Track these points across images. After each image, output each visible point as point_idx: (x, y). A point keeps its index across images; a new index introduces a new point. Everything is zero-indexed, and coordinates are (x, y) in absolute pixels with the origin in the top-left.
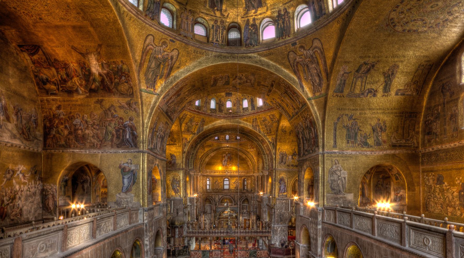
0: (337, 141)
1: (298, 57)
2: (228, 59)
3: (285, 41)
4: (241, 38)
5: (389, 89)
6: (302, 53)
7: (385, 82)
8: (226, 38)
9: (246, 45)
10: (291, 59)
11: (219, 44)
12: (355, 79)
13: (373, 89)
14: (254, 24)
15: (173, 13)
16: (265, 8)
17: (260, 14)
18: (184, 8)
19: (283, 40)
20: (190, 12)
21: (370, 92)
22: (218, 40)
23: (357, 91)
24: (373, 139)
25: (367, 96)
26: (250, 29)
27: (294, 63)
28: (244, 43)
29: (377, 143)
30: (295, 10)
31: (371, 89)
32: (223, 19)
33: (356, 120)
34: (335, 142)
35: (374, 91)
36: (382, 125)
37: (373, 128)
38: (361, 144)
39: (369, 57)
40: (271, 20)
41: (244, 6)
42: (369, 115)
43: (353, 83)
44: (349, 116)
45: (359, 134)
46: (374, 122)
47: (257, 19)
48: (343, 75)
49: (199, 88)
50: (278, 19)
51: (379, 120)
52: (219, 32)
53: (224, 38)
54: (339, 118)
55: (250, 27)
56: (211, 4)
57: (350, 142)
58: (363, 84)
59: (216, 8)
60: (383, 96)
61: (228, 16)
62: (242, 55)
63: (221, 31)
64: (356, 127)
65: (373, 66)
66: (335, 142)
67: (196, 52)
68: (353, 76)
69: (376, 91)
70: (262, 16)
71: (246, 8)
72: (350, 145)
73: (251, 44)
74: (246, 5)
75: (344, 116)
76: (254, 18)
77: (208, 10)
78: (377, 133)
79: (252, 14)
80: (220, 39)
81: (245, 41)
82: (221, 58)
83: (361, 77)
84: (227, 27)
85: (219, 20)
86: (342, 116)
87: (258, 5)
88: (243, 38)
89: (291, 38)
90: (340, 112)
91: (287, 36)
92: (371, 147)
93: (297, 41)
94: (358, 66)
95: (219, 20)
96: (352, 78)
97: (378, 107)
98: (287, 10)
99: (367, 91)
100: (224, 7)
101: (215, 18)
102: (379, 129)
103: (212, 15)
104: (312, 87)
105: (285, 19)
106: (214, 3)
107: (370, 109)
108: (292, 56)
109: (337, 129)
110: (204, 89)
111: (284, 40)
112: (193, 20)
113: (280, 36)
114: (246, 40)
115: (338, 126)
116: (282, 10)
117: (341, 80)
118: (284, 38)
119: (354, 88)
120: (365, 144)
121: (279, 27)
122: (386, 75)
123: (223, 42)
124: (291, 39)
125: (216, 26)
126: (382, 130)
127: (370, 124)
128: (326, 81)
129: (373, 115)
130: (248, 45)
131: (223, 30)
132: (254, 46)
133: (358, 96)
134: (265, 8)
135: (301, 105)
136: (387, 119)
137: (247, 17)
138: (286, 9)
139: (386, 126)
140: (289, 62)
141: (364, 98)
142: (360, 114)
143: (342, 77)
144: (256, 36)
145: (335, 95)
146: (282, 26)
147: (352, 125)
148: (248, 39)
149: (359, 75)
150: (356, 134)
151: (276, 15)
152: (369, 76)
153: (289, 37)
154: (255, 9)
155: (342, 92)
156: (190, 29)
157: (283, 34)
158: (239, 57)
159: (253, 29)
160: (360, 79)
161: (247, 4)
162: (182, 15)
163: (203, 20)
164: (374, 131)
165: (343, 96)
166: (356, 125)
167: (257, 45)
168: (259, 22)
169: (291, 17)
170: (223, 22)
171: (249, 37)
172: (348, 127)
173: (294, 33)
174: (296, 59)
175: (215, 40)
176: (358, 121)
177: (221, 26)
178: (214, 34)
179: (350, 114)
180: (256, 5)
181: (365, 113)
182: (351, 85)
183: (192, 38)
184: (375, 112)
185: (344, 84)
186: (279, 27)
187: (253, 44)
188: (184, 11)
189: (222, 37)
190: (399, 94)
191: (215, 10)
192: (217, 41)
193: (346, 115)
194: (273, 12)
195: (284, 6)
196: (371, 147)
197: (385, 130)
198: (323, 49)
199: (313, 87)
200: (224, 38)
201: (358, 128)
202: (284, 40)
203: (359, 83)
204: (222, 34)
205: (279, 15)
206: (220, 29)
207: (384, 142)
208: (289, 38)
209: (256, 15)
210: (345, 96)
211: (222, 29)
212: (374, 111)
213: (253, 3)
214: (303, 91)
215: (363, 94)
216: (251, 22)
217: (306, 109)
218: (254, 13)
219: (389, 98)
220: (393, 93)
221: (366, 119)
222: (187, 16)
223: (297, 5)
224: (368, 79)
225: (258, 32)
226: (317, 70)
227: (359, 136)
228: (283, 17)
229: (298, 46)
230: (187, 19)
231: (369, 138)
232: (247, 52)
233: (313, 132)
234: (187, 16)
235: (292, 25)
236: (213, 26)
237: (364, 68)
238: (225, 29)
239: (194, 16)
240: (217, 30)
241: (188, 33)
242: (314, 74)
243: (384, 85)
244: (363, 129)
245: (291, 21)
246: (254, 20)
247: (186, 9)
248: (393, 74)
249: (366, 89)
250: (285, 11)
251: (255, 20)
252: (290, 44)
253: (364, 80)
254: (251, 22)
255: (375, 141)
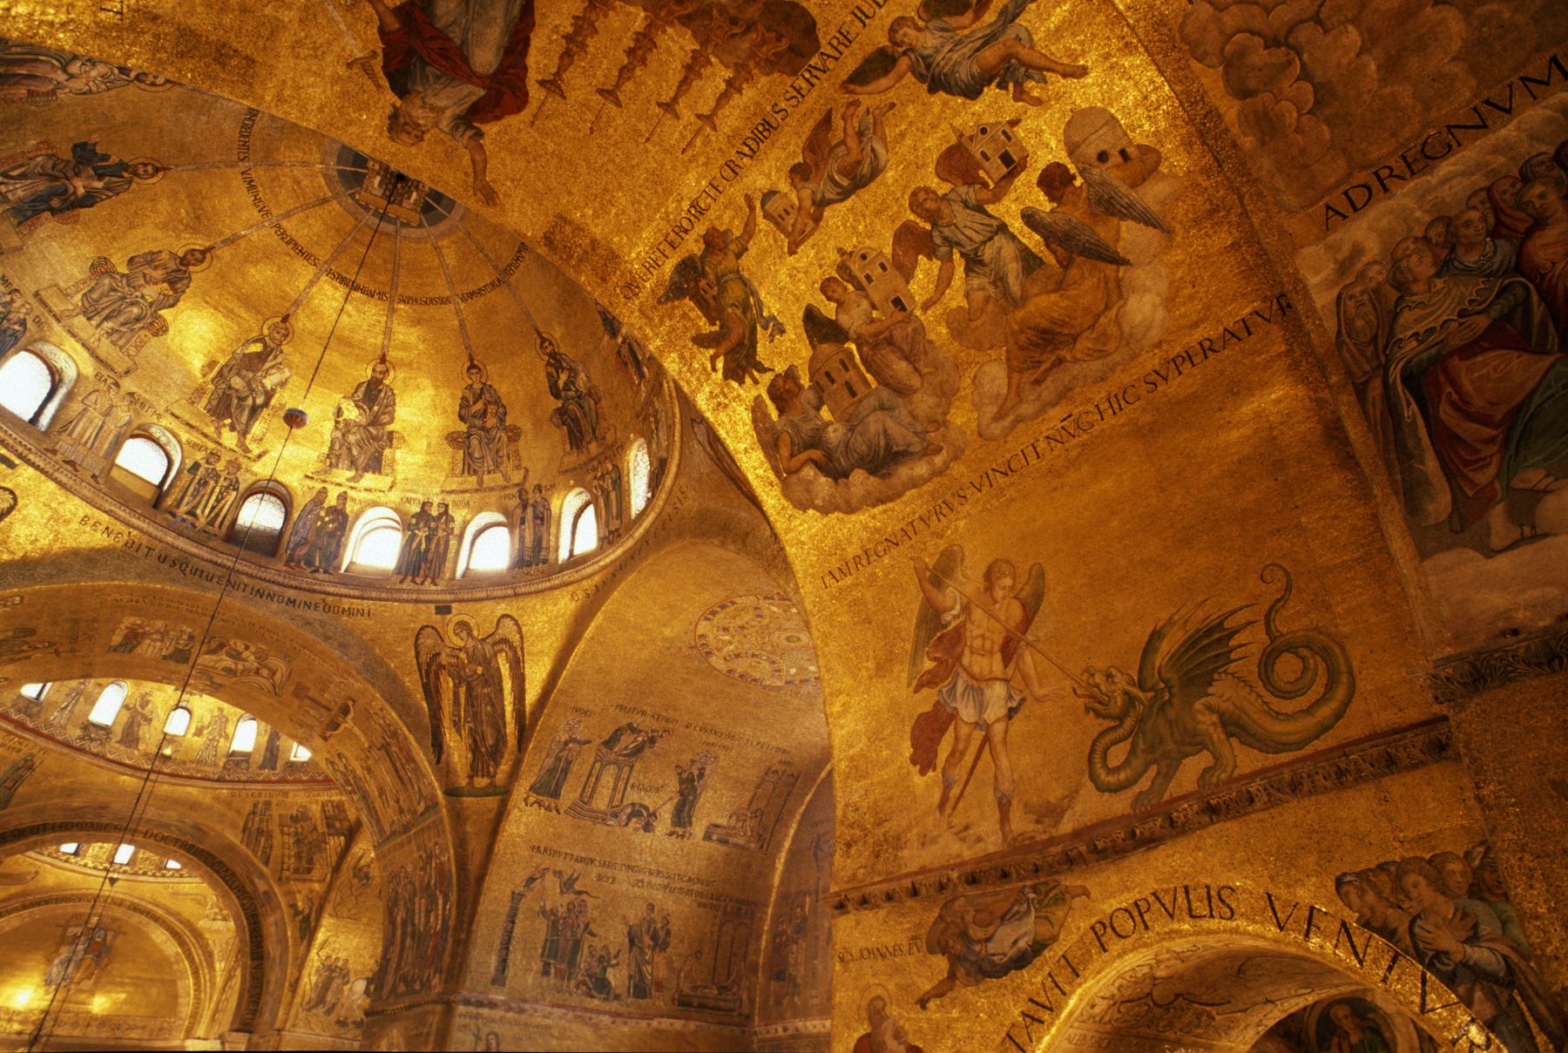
0: (510, 963)
1: (448, 650)
2: (208, 584)
3: (419, 591)
4: (282, 532)
5: (690, 817)
6: (461, 644)
7: (681, 793)
8: (229, 518)
9: (291, 559)
10: (423, 650)
11: (194, 526)
12: (598, 765)
13: (646, 808)
14: (339, 507)
15: (61, 380)
16: (389, 480)
17: (368, 490)
18: (110, 381)
19: (412, 586)
20: (128, 398)
21: (636, 813)
22: (199, 512)
23: (601, 803)
24: (625, 972)
25: (626, 825)
26: (320, 518)
27: (429, 665)
28: (284, 553)
29: (636, 986)
30: (472, 519)
31: (641, 805)
32: (241, 460)
33: (585, 897)
34: (503, 963)
35: (649, 815)
36: (659, 926)
37: (629, 934)
38: (585, 984)
39: (644, 713)
40: (398, 519)
41: (325, 449)
42: (625, 886)
43: (590, 774)
44: (566, 877)
45: (586, 945)
46: (635, 914)
47: (354, 500)
48: (566, 743)
49: (52, 644)
50: (417, 524)
51: (651, 907)
52: (209, 490)
53: (222, 514)
54: (532, 880)
55: (323, 513)
56: (218, 405)
57: (553, 971)
58: (621, 785)
59: (228, 421)
60: (671, 834)
61: (260, 456)
62: (265, 584)
63: (217, 490)
64: (581, 919)
65: (652, 741)
66: (503, 963)
67: (92, 522)
68: (594, 755)
69: (654, 814)
70: (370, 496)
71: (328, 456)
72: (552, 982)
73: (309, 563)
74: (332, 448)
75: (549, 877)
76: (345, 493)
77: (198, 414)
78: (641, 949)
79: (341, 480)
80: (207, 511)
81: (291, 546)
82: (183, 572)
83: (615, 763)
84: (243, 487)
85: (226, 457)
86: (543, 875)
87: (368, 464)
88: (286, 537)
89: (439, 588)
90: (538, 859)
91: (429, 580)
92: (617, 997)
93: (454, 605)
94: (612, 729)
95: (226, 457)
96: (592, 760)
97: (653, 867)
98: (450, 512)
99: (629, 810)
100: (257, 428)
101: (211, 445)
102: (647, 940)
103: (206, 436)
104: (470, 755)
105: (436, 529)
106: (229, 406)
107: (629, 867)
108: (429, 642)
109: (520, 916)
110: (73, 651)
111: (416, 587)
112: (129, 423)
113: (407, 570)
114: (298, 545)
115: (523, 906)
116: (435, 504)
117: (558, 759)
118: (418, 580)
119: (594, 790)
120: (601, 986)
121: (414, 545)
122: (685, 776)
123: (211, 523)
124: (437, 592)
125: (207, 469)
126: (656, 944)
127: (624, 917)
128: (515, 749)
129: (636, 889)
130: (299, 562)
131: (227, 488)
132: (317, 571)
133: (600, 818)
134: (389, 480)
135: (422, 804)
136: (678, 909)
137: (324, 481)
138: (447, 506)
139: (668, 933)
140: (417, 655)
141: (617, 829)
142: (600, 878)
143: (561, 751)
144: (334, 545)
145: (532, 799)
146: (423, 546)
147: (569, 910)
148: (305, 544)
149: (612, 757)
150: (577, 945)
151: (416, 509)
152: (637, 766)
153: (436, 584)
154: (357, 470)
155: (556, 794)
156: (106, 446)
157: (419, 568)
158: (249, 589)
159: (331, 521)
160: (612, 769)
161: (337, 447)
162: (93, 397)
163: (170, 436)
164: (632, 941)
165: (558, 811)
166: (581, 912)
167: (326, 572)
168: (357, 507)
169: (456, 532)
170: (239, 467)
171: (311, 537)
172: (555, 915)
173: (453, 578)
174: (438, 654)
175: (184, 508)
176: (590, 902)
177: (224, 475)
178: (191, 489)
179: (570, 873)
180: (362, 461)
181: (614, 879)
182: (584, 779)
183: (94, 477)
184: (642, 881)
185: (565, 771)
186: (414, 545)
187: (317, 564)
188: (105, 388)
189: (213, 508)
190: (715, 837)
191: (224, 425)
192: (192, 513)
193: (555, 873)
194: (408, 500)
195: (443, 496)
196: (617, 997)
197: (666, 945)
198: (522, 648)
199: (474, 754)
200: (222, 514)
201: (587, 926)
202: (416, 587)
203: (608, 779)
204: (218, 501)
205: (423, 514)
206: (216, 482)
207: (659, 985)
208: (433, 588)
209: (352, 488)
210: (562, 811)
211: (225, 484)
212: (640, 877)
213: (355, 452)
214: (438, 762)
215: (615, 815)
216: (332, 500)
217: (434, 822)
218: (348, 480)
219: (687, 843)
220: (698, 829)
221: (612, 900)
222: (112, 406)
223: (480, 510)
224: (634, 773)
225: (343, 535)
226: (493, 706)
227: (586, 951)
228: (433, 525)
229: (453, 618)
230: (107, 414)
231: (613, 966)
232: (286, 581)
233: (440, 912)
234: (112, 406)
235: (451, 555)
236: (196, 466)
237: (627, 741)
238: (236, 489)
239: (137, 413)
240: (206, 483)
241: (86, 456)
242: (484, 718)
243: (676, 801)
244: (601, 932)
245: (453, 543)
246: (343, 497)
247: (117, 385)
248: (701, 775)
249: (625, 803)
250: (442, 510)
251: (345, 499)
252: (433, 606)
253: (624, 776)
254: (332, 500)
255: (630, 977)
